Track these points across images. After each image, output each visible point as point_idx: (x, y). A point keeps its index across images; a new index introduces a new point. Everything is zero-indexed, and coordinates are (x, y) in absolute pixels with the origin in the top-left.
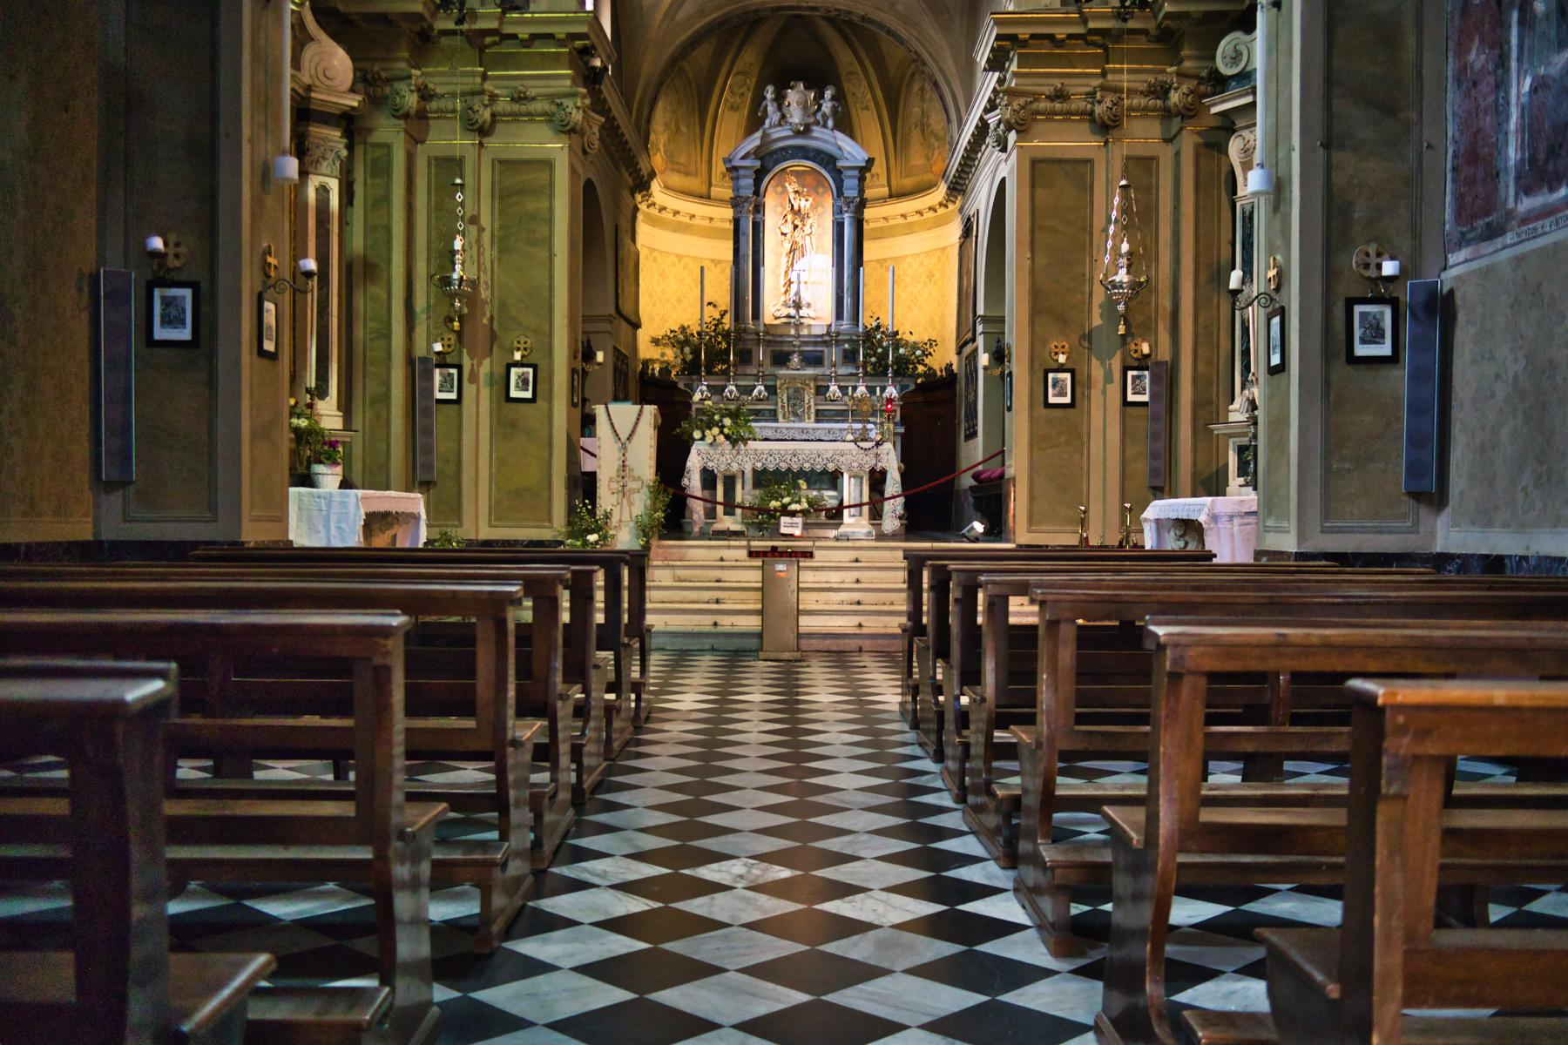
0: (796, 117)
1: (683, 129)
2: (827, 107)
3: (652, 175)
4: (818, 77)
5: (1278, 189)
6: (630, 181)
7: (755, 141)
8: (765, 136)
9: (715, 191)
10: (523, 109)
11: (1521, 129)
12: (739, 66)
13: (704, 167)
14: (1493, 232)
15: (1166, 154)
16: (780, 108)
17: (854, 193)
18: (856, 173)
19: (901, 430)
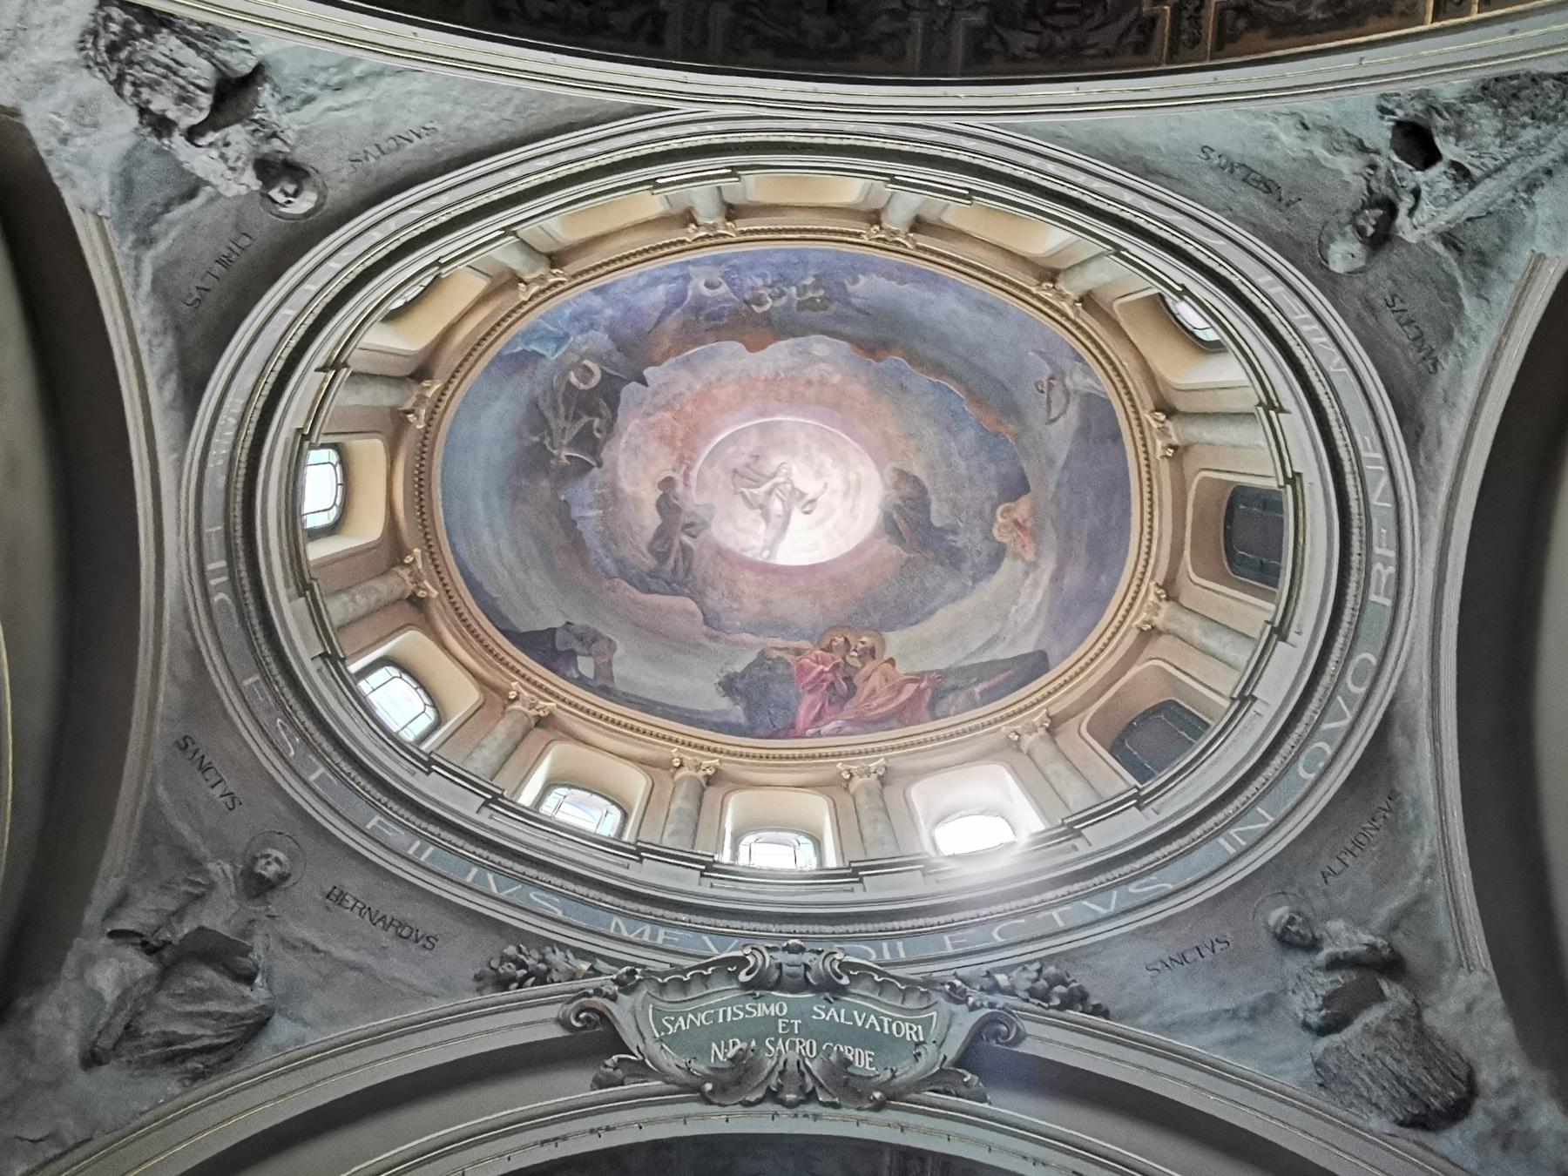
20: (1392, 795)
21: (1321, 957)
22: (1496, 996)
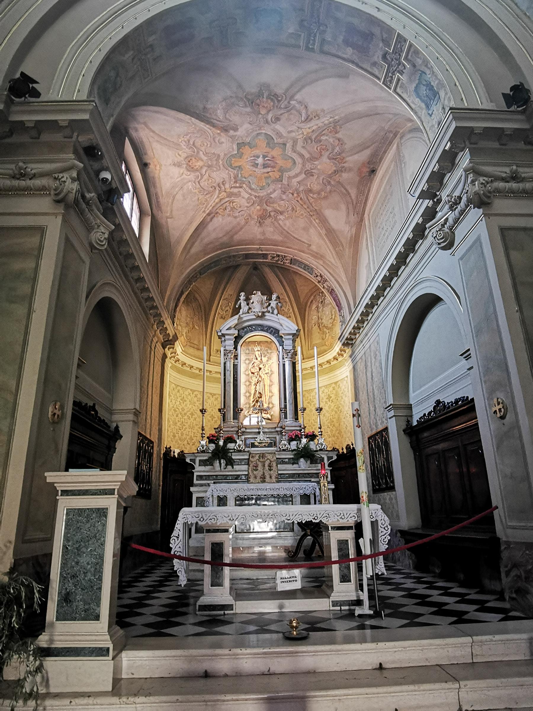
7: (234, 321)
12: (226, 295)
16: (248, 304)
17: (291, 348)
18: (291, 337)
19: (333, 486)
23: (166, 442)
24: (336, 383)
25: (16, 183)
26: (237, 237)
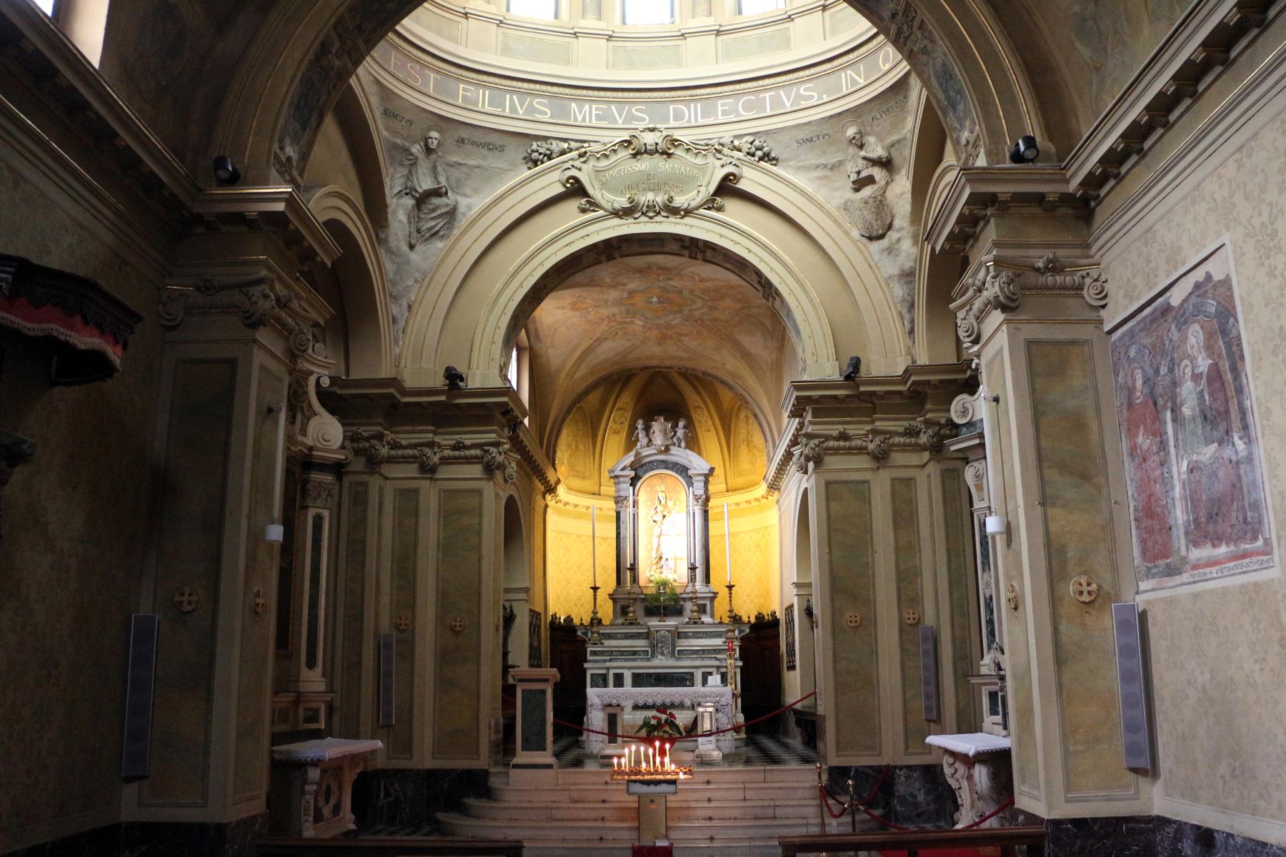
0: (658, 440)
1: (581, 447)
2: (680, 432)
3: (558, 482)
4: (674, 411)
5: (1009, 531)
6: (542, 488)
8: (638, 454)
9: (604, 490)
10: (462, 453)
11: (1184, 498)
12: (619, 405)
13: (596, 473)
14: (1171, 571)
15: (921, 476)
16: (647, 435)
17: (701, 492)
18: (702, 478)
19: (740, 663)
20: (906, 97)
21: (863, 153)
22: (909, 195)
23: (552, 610)
24: (766, 528)
25: (456, 453)
26: (631, 356)
